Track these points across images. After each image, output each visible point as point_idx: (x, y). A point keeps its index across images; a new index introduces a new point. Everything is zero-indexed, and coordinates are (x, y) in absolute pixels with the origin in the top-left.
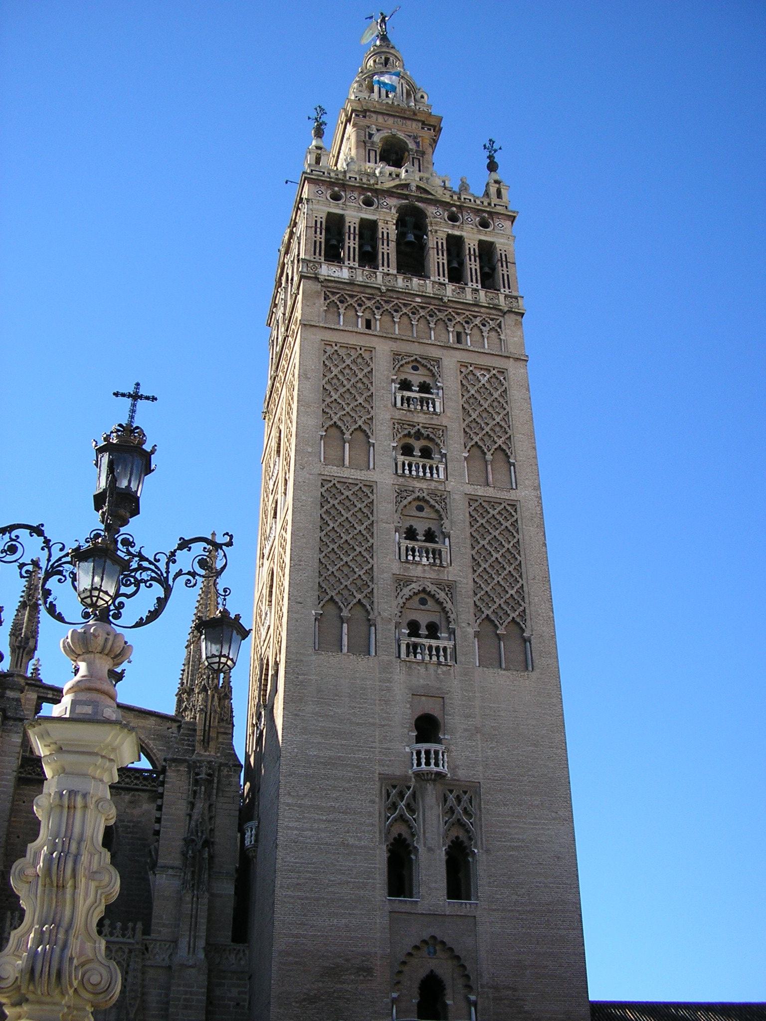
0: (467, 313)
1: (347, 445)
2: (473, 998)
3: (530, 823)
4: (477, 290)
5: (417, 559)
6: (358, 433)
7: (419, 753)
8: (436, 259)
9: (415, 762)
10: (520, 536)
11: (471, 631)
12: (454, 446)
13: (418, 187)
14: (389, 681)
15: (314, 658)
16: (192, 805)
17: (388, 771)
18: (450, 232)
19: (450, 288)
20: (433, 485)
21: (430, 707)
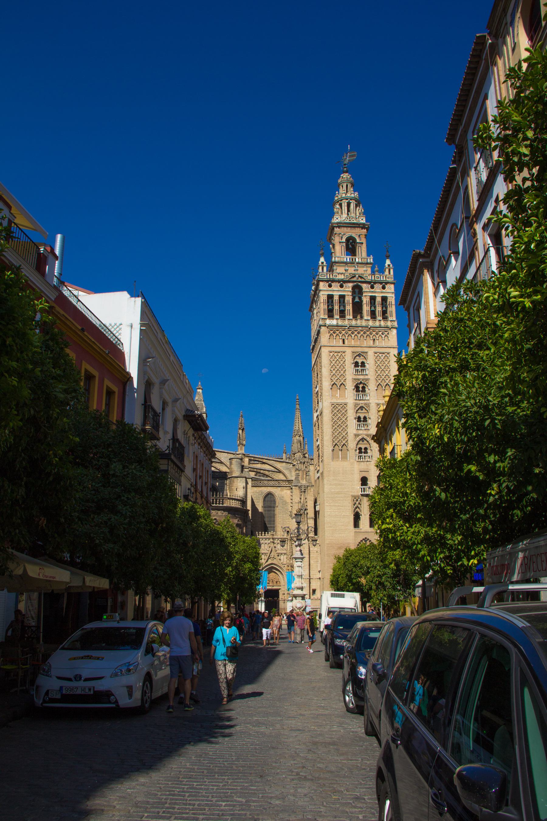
4: (380, 320)
8: (366, 308)
17: (353, 494)
18: (371, 294)
20: (366, 402)
21: (364, 474)
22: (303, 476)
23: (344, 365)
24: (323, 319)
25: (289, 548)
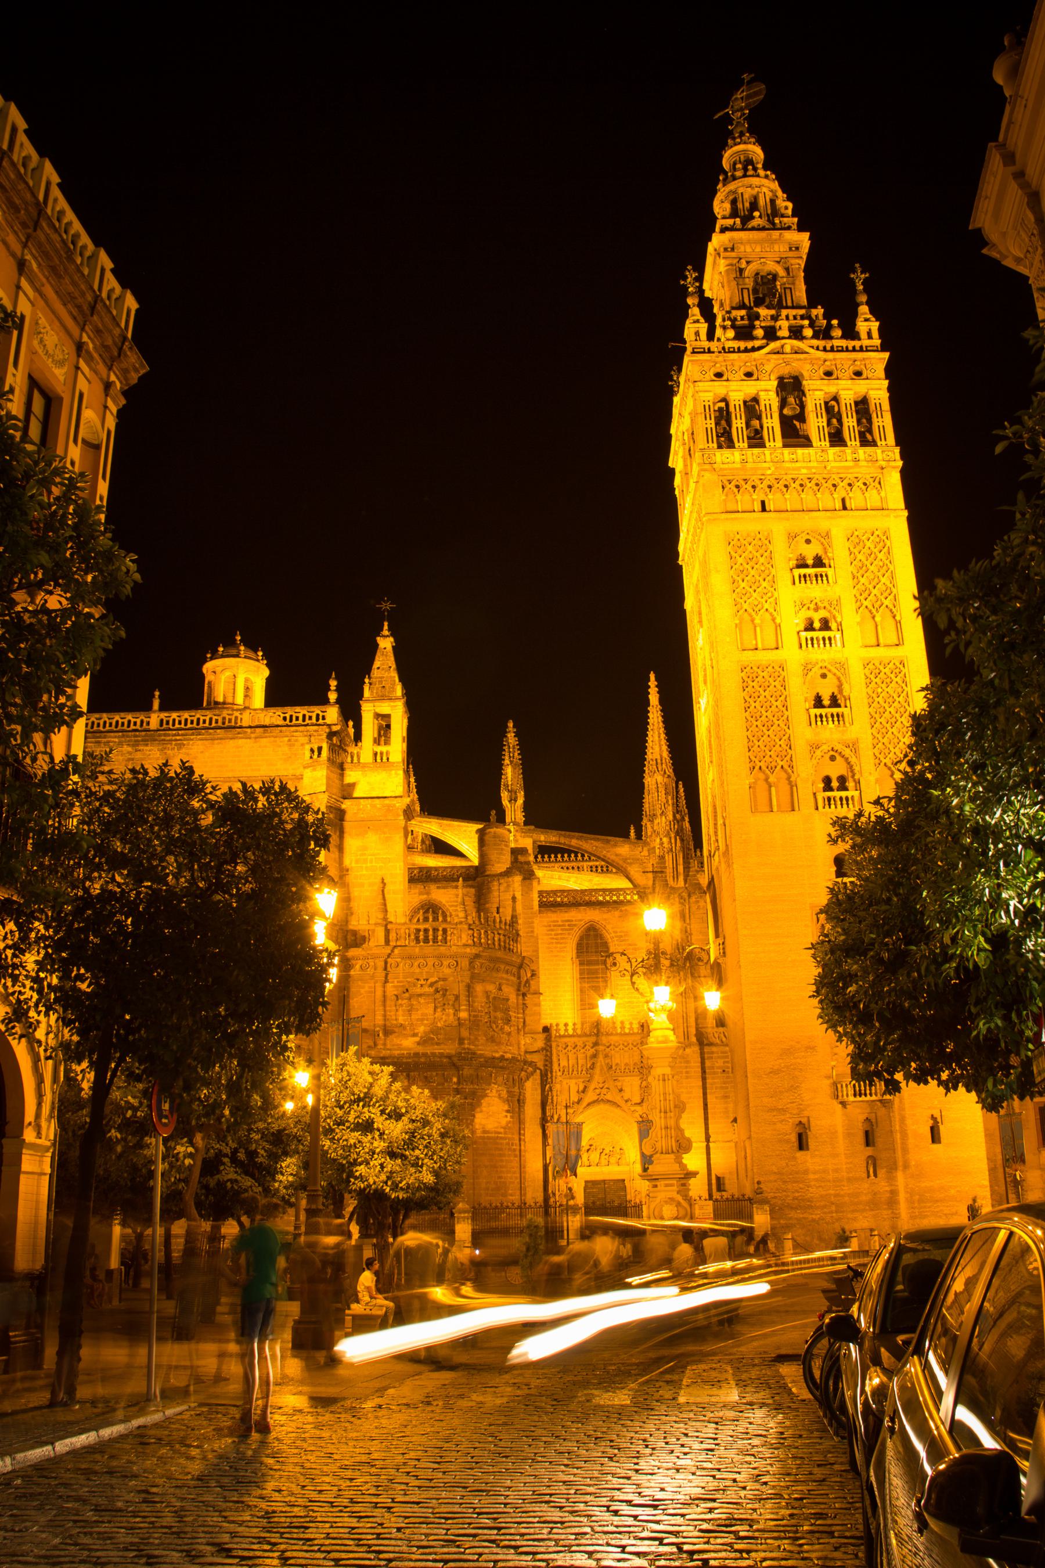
0: (849, 476)
1: (758, 629)
6: (767, 615)
8: (815, 424)
11: (872, 779)
19: (833, 451)
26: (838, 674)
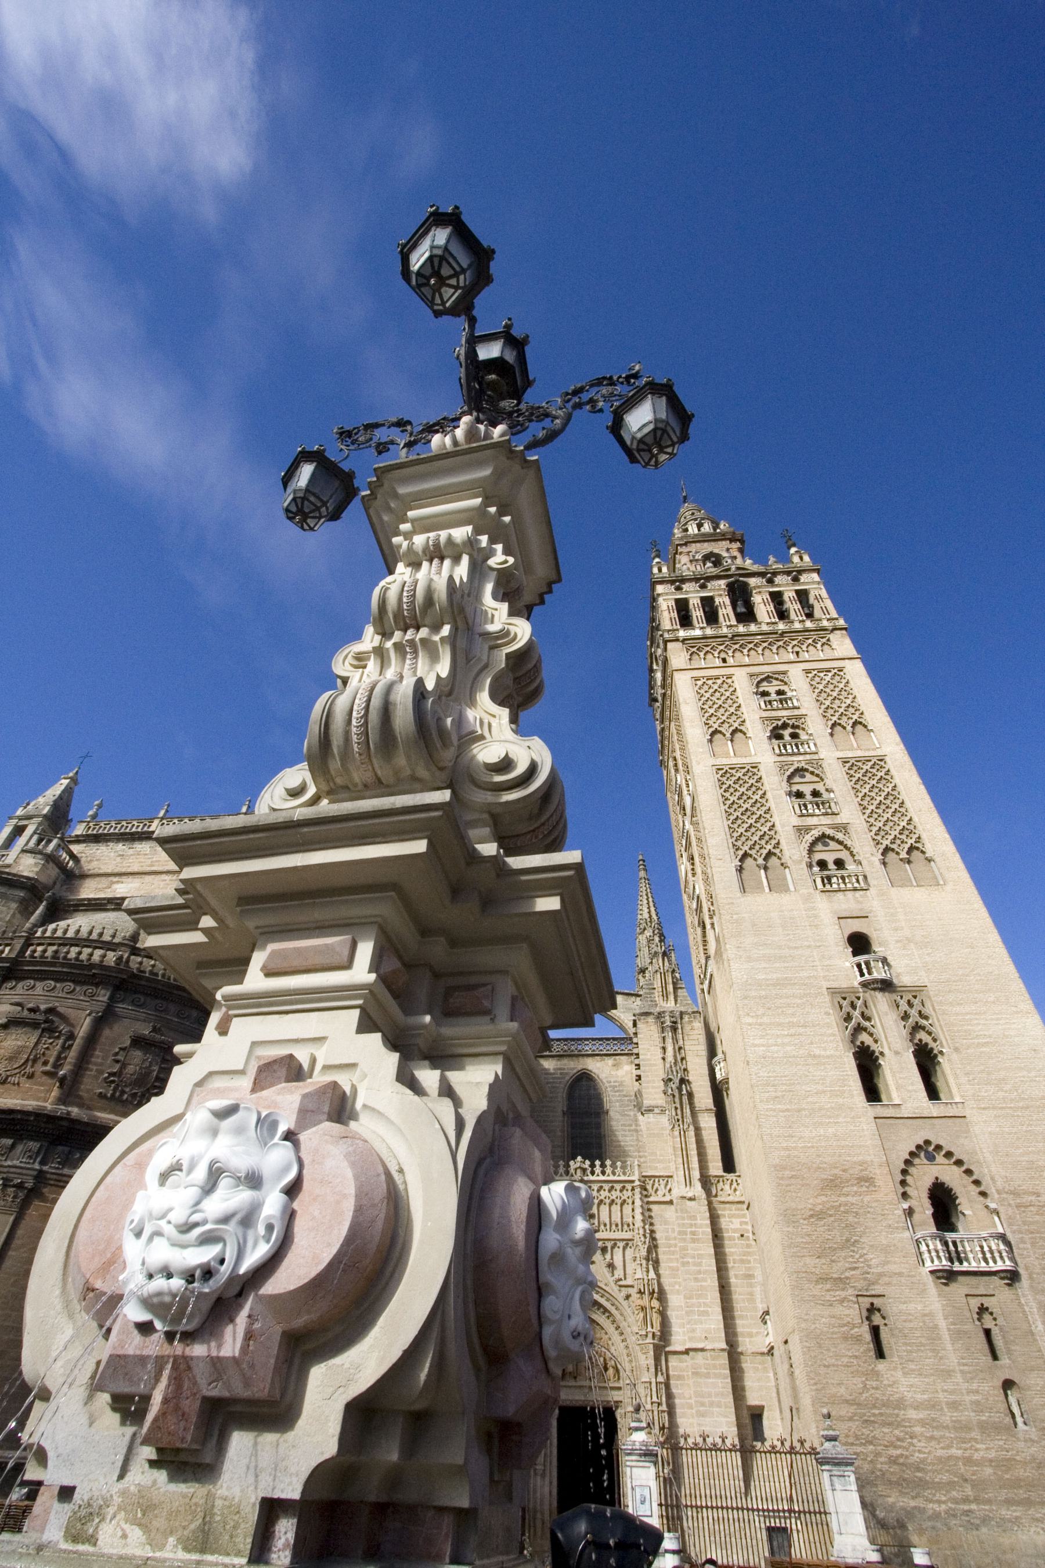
2: (993, 1206)
3: (992, 1019)
4: (803, 621)
5: (810, 811)
7: (859, 966)
8: (763, 609)
9: (858, 973)
10: (897, 780)
12: (816, 726)
13: (738, 569)
14: (813, 908)
15: (742, 900)
16: (664, 1049)
21: (856, 926)
22: (664, 987)
23: (733, 697)
24: (669, 631)
25: (639, 1217)
26: (816, 772)
